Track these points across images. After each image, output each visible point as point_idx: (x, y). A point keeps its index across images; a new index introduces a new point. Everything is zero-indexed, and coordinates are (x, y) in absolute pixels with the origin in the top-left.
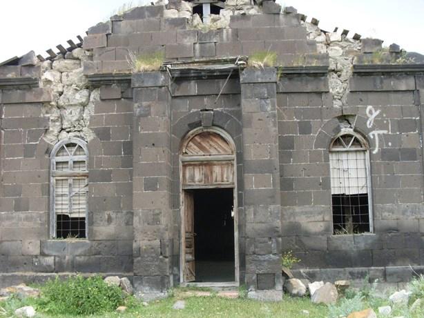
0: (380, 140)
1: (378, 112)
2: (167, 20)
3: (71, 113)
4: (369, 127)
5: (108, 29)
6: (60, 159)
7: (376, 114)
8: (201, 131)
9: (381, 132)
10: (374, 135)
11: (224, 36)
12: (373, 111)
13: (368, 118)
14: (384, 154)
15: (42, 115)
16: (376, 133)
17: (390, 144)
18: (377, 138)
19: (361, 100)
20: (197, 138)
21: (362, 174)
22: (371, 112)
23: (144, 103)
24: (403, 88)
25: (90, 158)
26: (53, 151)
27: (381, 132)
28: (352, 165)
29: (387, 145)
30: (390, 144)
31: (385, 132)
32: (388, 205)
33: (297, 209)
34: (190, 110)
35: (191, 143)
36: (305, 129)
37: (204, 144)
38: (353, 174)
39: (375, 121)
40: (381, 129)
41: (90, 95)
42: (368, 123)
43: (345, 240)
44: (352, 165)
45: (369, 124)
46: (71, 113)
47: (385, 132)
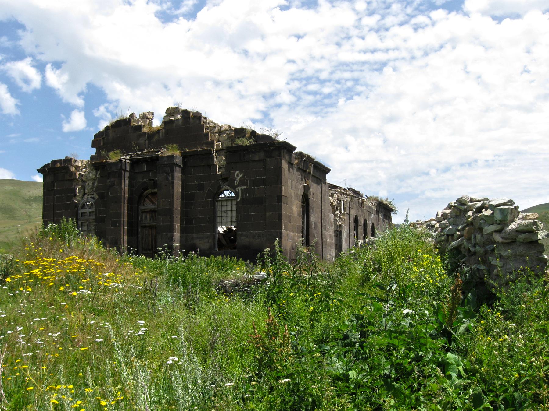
0: (242, 193)
1: (242, 175)
2: (132, 127)
3: (88, 184)
4: (236, 184)
5: (103, 135)
6: (83, 211)
7: (240, 176)
8: (150, 192)
9: (243, 187)
10: (238, 190)
11: (161, 135)
12: (239, 174)
13: (236, 179)
14: (243, 201)
15: (73, 186)
16: (240, 188)
17: (247, 195)
18: (240, 191)
19: (232, 168)
20: (149, 196)
21: (235, 214)
22: (238, 175)
23: (112, 179)
24: (257, 158)
25: (96, 210)
26: (80, 206)
27: (243, 187)
28: (229, 208)
29: (246, 195)
30: (247, 195)
31: (245, 187)
32: (245, 232)
33: (195, 235)
34: (143, 180)
35: (146, 199)
36: (201, 187)
37: (153, 200)
38: (230, 214)
39: (240, 180)
40: (243, 185)
41: (97, 174)
42: (236, 182)
43: (417, 265)
44: (229, 208)
45: (236, 183)
46: (88, 184)
47: (245, 187)
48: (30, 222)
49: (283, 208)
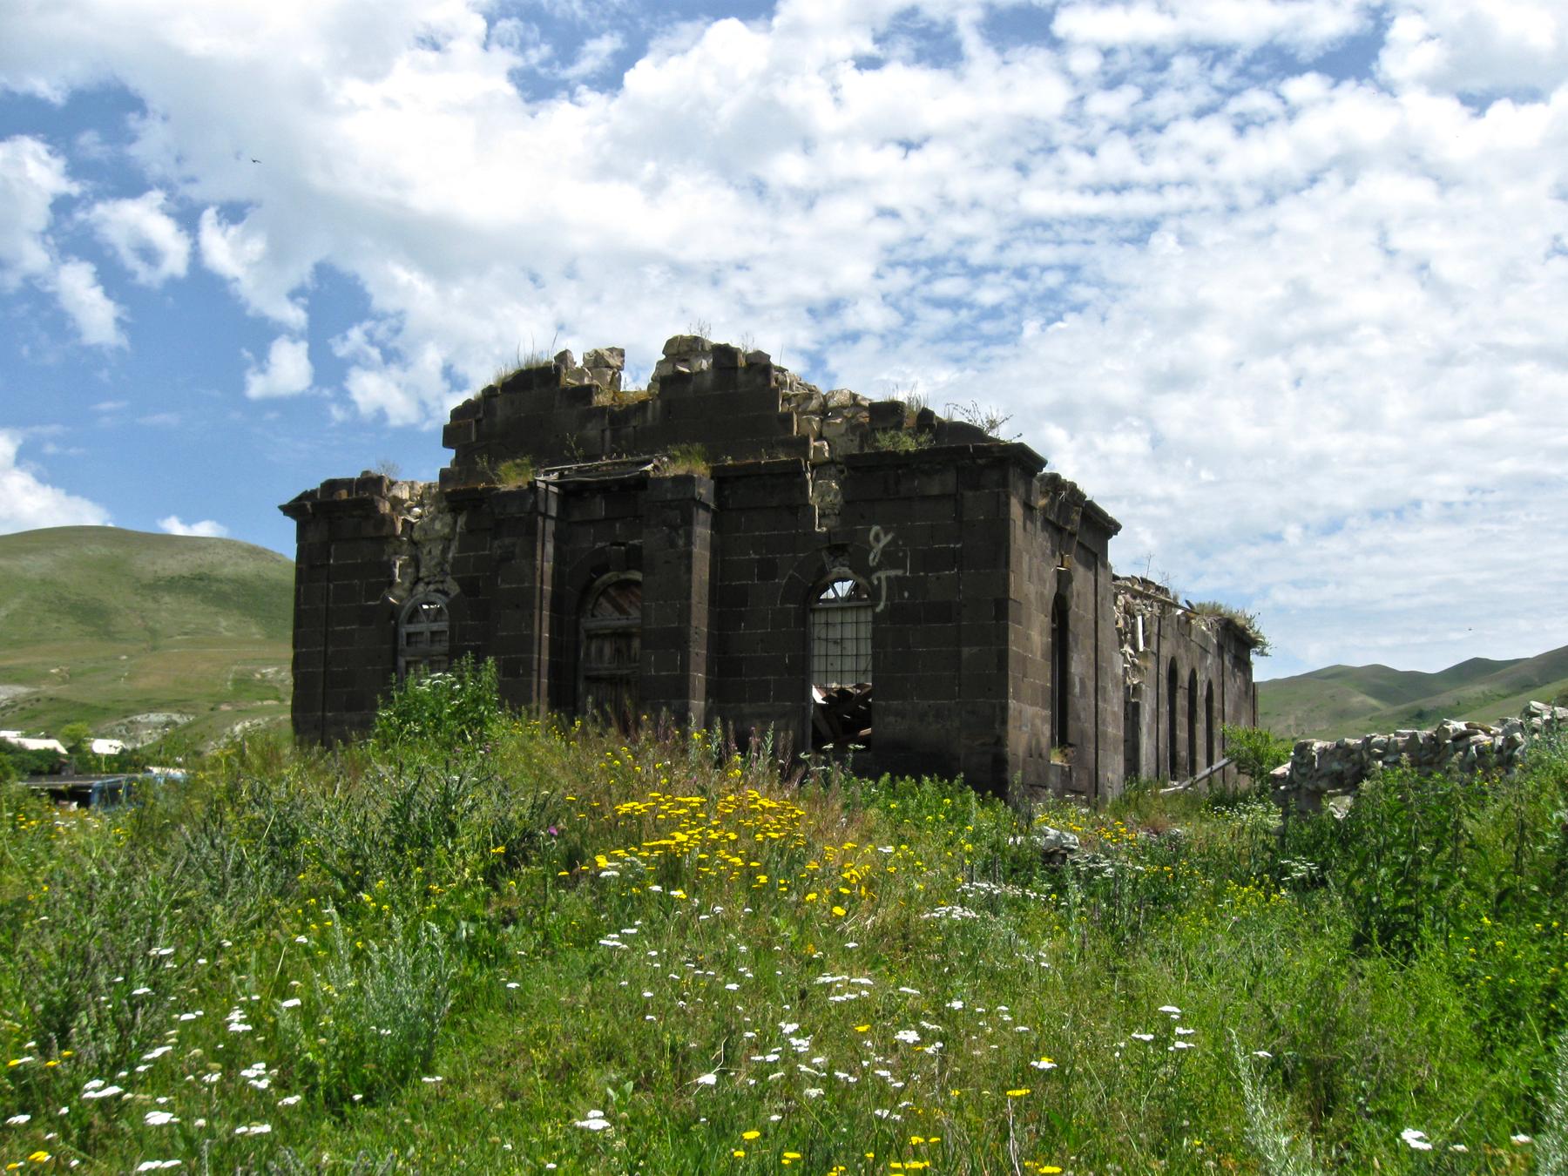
0: (889, 588)
1: (889, 537)
2: (565, 390)
3: (430, 552)
4: (871, 564)
5: (478, 412)
6: (412, 628)
7: (885, 540)
8: (615, 579)
9: (893, 573)
10: (879, 579)
11: (649, 414)
12: (882, 536)
13: (872, 548)
14: (893, 612)
15: (385, 558)
16: (883, 575)
17: (906, 594)
18: (884, 584)
19: (863, 517)
20: (612, 591)
21: (866, 648)
22: (877, 538)
23: (507, 541)
24: (935, 490)
25: (451, 627)
26: (403, 614)
27: (893, 573)
28: (849, 632)
30: (906, 594)
31: (899, 573)
32: (895, 703)
34: (594, 544)
35: (602, 600)
36: (768, 570)
37: (621, 602)
38: (850, 648)
39: (884, 552)
41: (455, 522)
42: (871, 557)
44: (849, 632)
45: (872, 559)
46: (430, 552)
47: (899, 573)
48: (154, 648)
49: (1012, 637)
